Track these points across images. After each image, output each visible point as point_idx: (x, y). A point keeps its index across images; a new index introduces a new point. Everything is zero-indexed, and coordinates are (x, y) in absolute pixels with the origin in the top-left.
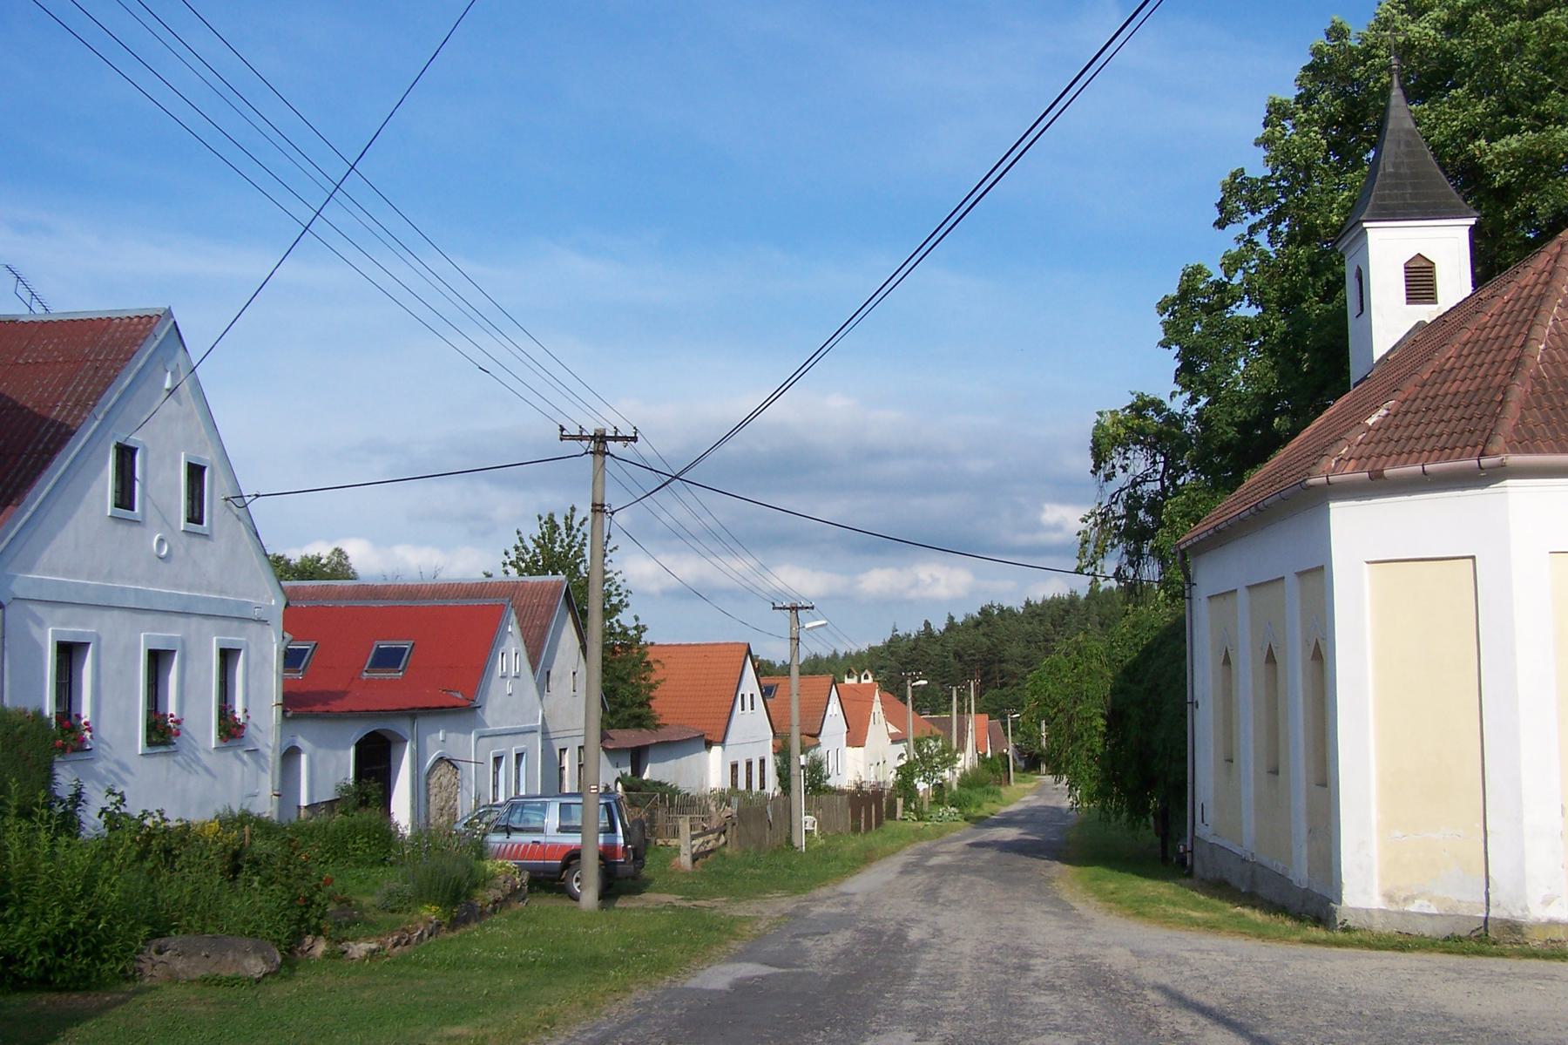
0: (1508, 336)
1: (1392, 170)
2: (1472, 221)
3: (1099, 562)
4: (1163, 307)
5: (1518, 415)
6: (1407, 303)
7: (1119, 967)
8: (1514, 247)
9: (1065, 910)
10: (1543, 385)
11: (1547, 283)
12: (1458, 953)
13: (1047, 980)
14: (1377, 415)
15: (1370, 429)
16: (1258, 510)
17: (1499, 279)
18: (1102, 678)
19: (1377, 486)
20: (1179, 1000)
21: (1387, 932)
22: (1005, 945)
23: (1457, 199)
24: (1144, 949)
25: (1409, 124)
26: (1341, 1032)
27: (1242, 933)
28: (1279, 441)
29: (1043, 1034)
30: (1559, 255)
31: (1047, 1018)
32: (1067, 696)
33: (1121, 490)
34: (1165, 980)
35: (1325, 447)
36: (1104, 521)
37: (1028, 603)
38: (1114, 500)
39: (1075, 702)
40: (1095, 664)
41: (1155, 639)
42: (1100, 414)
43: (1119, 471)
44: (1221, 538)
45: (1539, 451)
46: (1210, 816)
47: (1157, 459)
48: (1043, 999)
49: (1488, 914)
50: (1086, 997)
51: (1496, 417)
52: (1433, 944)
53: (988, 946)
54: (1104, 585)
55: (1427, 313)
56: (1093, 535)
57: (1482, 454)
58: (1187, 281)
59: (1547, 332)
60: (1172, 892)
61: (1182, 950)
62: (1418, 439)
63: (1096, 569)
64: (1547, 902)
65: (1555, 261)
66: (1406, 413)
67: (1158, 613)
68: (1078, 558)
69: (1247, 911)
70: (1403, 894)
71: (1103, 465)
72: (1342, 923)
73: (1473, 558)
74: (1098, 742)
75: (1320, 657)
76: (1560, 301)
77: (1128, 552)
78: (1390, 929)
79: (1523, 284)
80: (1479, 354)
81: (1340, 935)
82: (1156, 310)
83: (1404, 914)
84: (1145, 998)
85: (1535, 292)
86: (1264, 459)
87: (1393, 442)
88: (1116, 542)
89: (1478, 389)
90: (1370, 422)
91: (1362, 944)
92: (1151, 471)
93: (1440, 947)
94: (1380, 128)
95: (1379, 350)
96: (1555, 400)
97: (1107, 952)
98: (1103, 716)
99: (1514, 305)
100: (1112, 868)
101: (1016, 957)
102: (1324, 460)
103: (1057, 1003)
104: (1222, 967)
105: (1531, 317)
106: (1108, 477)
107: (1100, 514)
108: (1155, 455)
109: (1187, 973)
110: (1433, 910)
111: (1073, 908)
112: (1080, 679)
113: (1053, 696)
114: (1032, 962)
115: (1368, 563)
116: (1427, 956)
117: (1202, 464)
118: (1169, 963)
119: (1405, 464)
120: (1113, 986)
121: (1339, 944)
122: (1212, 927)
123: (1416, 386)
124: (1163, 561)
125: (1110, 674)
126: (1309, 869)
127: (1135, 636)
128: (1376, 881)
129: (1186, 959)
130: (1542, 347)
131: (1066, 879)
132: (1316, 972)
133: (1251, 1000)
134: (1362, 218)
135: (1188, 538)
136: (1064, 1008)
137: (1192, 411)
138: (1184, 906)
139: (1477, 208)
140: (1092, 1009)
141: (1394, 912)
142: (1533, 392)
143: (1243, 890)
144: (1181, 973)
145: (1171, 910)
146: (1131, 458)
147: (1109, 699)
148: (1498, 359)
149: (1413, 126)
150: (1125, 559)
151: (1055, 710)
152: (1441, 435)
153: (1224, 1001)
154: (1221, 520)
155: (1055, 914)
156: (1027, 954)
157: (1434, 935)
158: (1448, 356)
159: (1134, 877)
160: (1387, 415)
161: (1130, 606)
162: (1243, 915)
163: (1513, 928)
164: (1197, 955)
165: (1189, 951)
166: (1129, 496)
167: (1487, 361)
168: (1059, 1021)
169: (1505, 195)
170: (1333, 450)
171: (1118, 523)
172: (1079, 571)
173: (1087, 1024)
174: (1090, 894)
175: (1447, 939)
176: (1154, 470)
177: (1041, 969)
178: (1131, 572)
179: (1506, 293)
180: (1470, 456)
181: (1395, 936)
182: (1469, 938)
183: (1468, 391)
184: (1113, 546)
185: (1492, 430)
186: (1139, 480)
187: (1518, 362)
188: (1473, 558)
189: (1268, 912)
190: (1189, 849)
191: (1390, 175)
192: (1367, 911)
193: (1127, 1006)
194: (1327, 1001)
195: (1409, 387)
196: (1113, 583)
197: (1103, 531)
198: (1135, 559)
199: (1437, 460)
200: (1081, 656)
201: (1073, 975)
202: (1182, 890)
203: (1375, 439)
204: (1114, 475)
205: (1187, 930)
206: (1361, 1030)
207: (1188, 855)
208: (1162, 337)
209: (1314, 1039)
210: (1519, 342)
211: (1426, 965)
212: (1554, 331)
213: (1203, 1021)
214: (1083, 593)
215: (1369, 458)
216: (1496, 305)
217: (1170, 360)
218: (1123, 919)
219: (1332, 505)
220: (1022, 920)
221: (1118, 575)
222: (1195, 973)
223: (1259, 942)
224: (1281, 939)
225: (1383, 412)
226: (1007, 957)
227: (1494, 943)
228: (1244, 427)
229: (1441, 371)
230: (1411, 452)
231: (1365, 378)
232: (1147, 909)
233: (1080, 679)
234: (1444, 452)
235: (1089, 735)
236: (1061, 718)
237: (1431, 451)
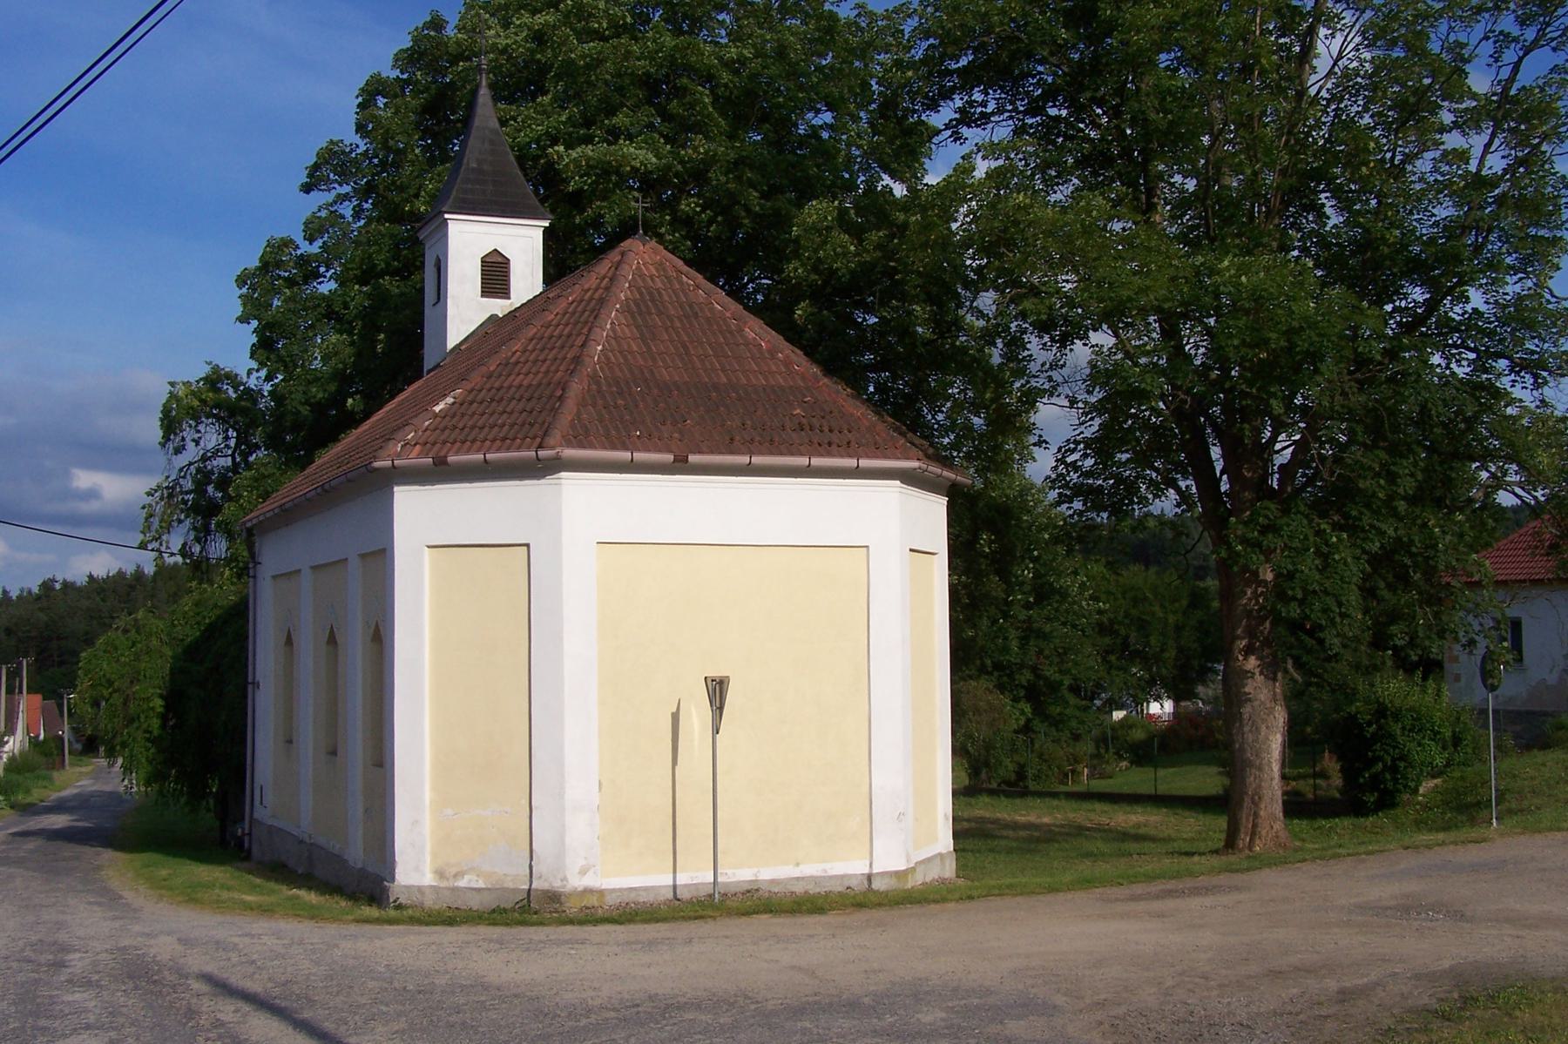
0: (569, 336)
1: (475, 165)
2: (546, 224)
3: (164, 537)
4: (241, 281)
5: (575, 411)
6: (482, 296)
7: (164, 957)
8: (584, 252)
9: (111, 899)
10: (598, 383)
11: (607, 289)
12: (501, 924)
13: (84, 975)
14: (444, 402)
15: (436, 415)
16: (326, 491)
17: (568, 280)
18: (161, 657)
19: (440, 472)
20: (224, 988)
21: (437, 907)
22: (41, 941)
23: (535, 201)
24: (192, 936)
25: (495, 124)
26: (384, 1009)
27: (296, 915)
28: (352, 421)
29: (71, 1035)
30: (619, 264)
31: (78, 1017)
32: (122, 676)
33: (191, 464)
34: (210, 968)
35: (395, 431)
36: (171, 496)
37: (91, 576)
38: (182, 474)
39: (132, 682)
40: (155, 642)
41: (219, 617)
42: (172, 384)
43: (191, 446)
44: (288, 516)
45: (592, 447)
46: (269, 797)
47: (230, 434)
48: (77, 996)
49: (531, 885)
50: (124, 991)
51: (554, 412)
52: (480, 918)
53: (21, 943)
54: (170, 560)
55: (499, 307)
56: (159, 509)
57: (540, 446)
58: (271, 252)
59: (605, 334)
60: (228, 875)
61: (231, 936)
62: (482, 428)
63: (161, 545)
64: (583, 872)
65: (616, 269)
66: (471, 403)
67: (223, 591)
68: (142, 532)
69: (302, 893)
70: (454, 870)
71: (172, 437)
72: (395, 901)
73: (528, 545)
74: (155, 723)
75: (380, 639)
76: (618, 306)
77: (195, 528)
78: (440, 905)
79: (586, 287)
80: (542, 350)
81: (392, 913)
82: (235, 285)
83: (454, 890)
84: (188, 989)
85: (597, 296)
86: (335, 439)
87: (457, 429)
88: (182, 517)
89: (540, 384)
90: (437, 409)
91: (414, 921)
92: (222, 446)
93: (486, 919)
94: (467, 121)
95: (453, 340)
96: (608, 398)
97: (152, 942)
98: (161, 696)
99: (576, 307)
100: (168, 854)
101: (51, 953)
102: (391, 443)
103: (91, 999)
104: (272, 951)
105: (591, 319)
106: (178, 451)
107: (167, 488)
108: (227, 430)
109: (235, 960)
110: (481, 884)
111: (121, 897)
112: (137, 658)
113: (108, 676)
114: (71, 956)
115: (428, 547)
116: (473, 929)
117: (273, 442)
118: (217, 949)
119: (468, 452)
120: (156, 978)
121: (391, 922)
122: (265, 911)
123: (483, 377)
124: (230, 536)
125: (170, 653)
126: (364, 850)
127: (198, 614)
128: (428, 858)
129: (236, 945)
130: (600, 348)
131: (116, 867)
132: (365, 951)
133: (297, 983)
134: (444, 209)
135: (252, 518)
136: (99, 1004)
137: (267, 388)
138: (239, 891)
139: (553, 211)
140: (130, 1003)
141: (443, 888)
142: (589, 390)
143: (300, 872)
144: (229, 959)
145: (225, 895)
146: (203, 431)
147: (167, 678)
148: (560, 356)
149: (497, 125)
150: (192, 535)
151: (110, 690)
152: (503, 425)
153: (270, 985)
154: (287, 499)
155: (99, 904)
156: (66, 949)
157: (481, 909)
158: (514, 350)
159: (188, 862)
160: (454, 404)
161: (194, 584)
162: (297, 897)
163: (553, 897)
164: (247, 940)
165: (240, 936)
166: (198, 470)
167: (549, 357)
168: (92, 1018)
169: (577, 200)
170: (399, 435)
171: (186, 498)
172: (143, 546)
173: (121, 1020)
174: (142, 882)
175: (494, 911)
176: (226, 445)
177: (78, 963)
178: (197, 549)
179: (571, 294)
180: (529, 448)
181: (444, 911)
182: (513, 910)
183: (530, 385)
184: (180, 522)
185: (550, 424)
186: (209, 454)
187: (577, 360)
188: (528, 545)
189: (323, 894)
190: (247, 832)
191: (473, 169)
192: (420, 889)
193: (168, 998)
194: (373, 979)
195: (476, 379)
196: (179, 559)
197: (170, 505)
198: (202, 535)
199: (498, 450)
200: (139, 634)
201: (113, 968)
202: (237, 874)
203: (441, 426)
204: (184, 449)
205: (240, 915)
206: (404, 1005)
207: (246, 839)
208: (239, 310)
209: (357, 1018)
210: (579, 342)
211: (471, 938)
212: (611, 334)
213: (246, 1008)
214: (149, 569)
215: (434, 444)
216: (562, 305)
217: (247, 335)
218: (174, 906)
219: (396, 489)
220: (63, 913)
221: (184, 552)
222: (244, 959)
223: (312, 923)
224: (335, 920)
225: (450, 400)
226: (42, 954)
227: (536, 913)
228: (319, 408)
229: (506, 365)
230: (474, 441)
231: (438, 366)
232: (199, 895)
233: (137, 658)
234: (505, 442)
235: (146, 717)
236: (117, 699)
237: (493, 441)
